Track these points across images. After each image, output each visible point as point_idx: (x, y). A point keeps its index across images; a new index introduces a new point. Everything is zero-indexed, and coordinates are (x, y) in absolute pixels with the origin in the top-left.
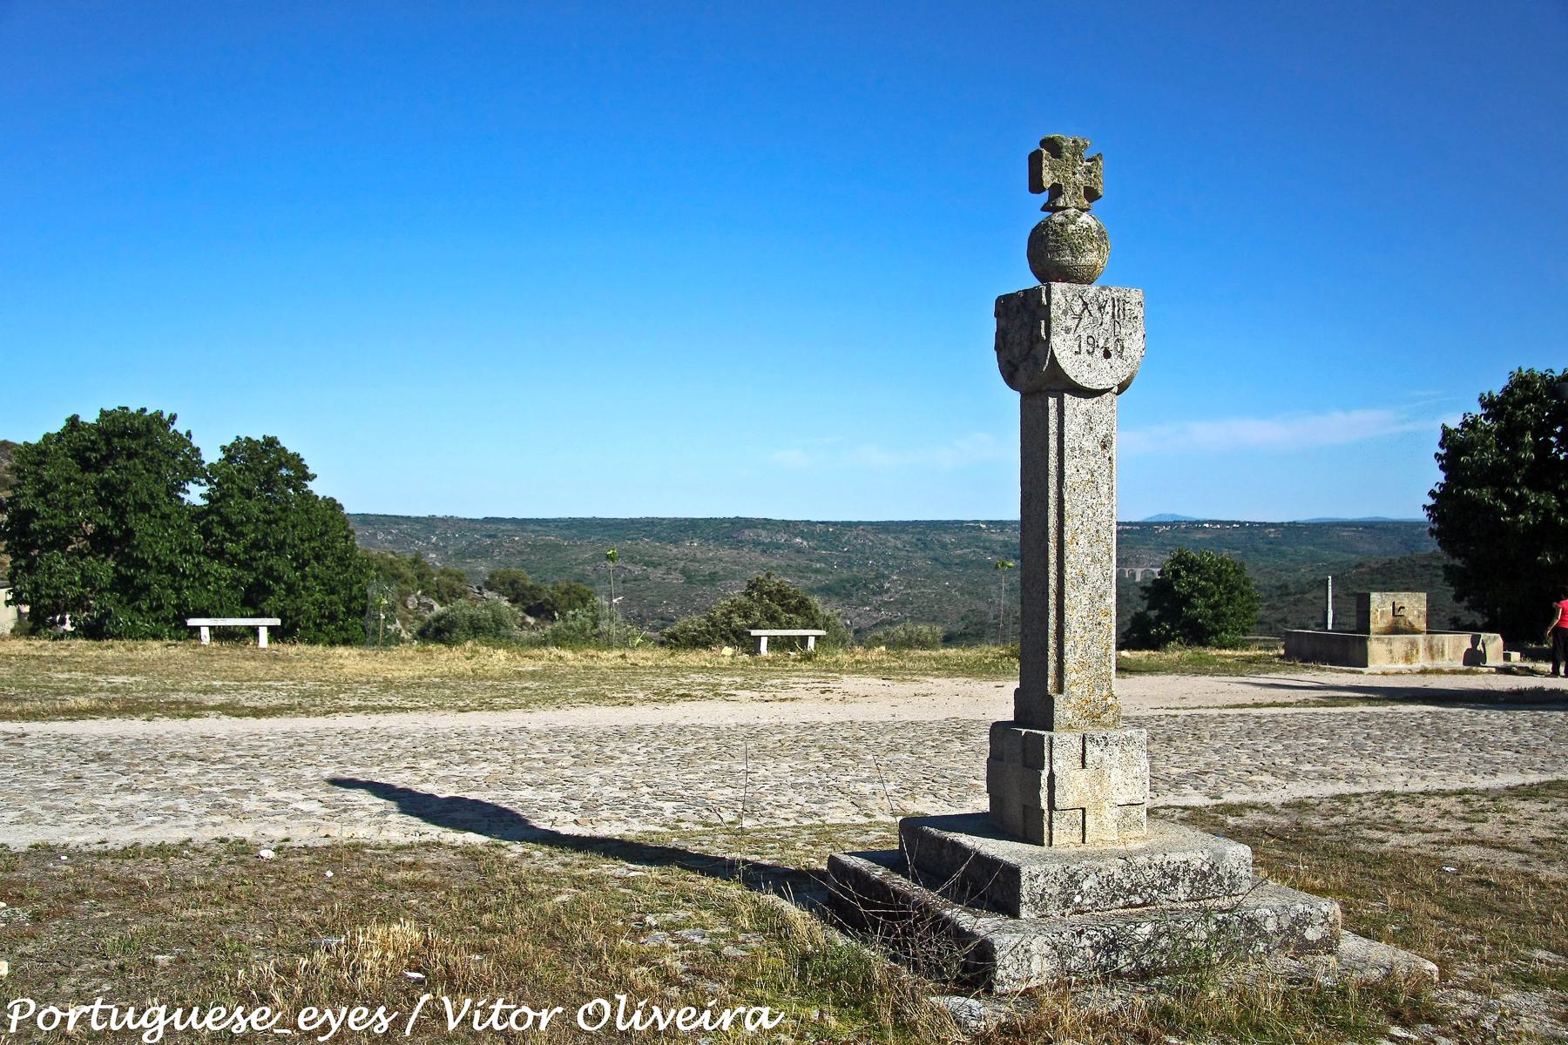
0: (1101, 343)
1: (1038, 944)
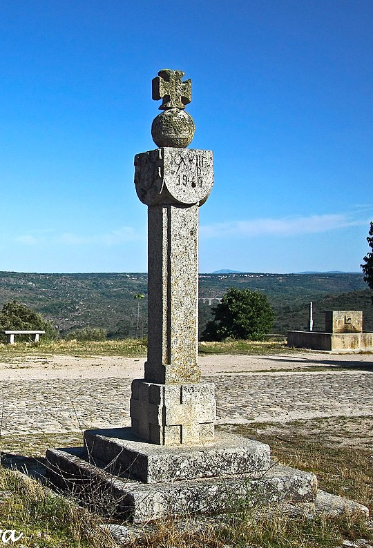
0: (191, 179)
1: (157, 497)
